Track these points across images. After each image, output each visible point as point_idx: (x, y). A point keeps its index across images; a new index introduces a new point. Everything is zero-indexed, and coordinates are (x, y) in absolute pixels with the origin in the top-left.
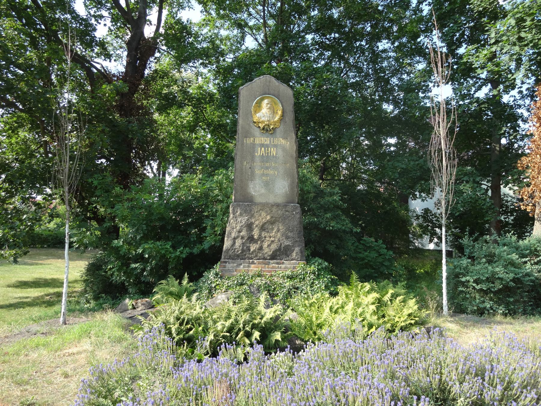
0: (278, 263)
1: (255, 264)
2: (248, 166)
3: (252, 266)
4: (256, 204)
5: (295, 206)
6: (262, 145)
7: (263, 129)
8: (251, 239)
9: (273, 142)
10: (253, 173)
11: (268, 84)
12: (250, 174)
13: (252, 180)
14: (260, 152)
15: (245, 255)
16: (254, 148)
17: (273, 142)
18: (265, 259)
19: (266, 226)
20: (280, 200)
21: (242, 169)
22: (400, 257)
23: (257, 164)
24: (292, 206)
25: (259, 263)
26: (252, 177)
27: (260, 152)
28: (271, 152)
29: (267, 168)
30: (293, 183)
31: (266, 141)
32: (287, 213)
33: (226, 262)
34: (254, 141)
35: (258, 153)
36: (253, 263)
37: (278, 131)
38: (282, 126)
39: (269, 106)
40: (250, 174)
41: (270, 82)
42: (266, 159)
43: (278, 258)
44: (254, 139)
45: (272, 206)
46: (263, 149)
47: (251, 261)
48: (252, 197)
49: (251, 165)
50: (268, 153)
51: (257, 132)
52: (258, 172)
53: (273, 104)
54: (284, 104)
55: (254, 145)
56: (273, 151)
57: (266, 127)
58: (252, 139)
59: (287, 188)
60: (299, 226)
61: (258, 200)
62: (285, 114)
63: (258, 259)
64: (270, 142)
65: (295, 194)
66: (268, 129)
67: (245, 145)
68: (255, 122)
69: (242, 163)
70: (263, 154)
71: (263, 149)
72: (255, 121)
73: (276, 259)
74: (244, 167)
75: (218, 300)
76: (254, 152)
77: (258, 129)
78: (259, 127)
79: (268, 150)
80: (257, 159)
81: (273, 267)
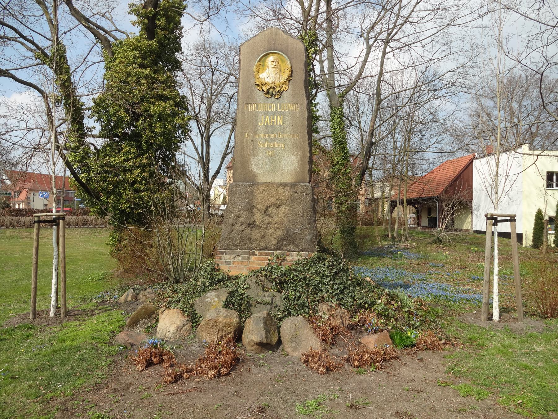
1: (256, 255)
2: (250, 139)
3: (252, 257)
4: (258, 184)
5: (305, 186)
6: (266, 113)
7: (268, 92)
8: (252, 225)
9: (280, 109)
10: (255, 146)
11: (273, 37)
12: (252, 148)
13: (254, 155)
14: (264, 121)
16: (256, 116)
17: (280, 109)
18: (266, 248)
19: (270, 210)
20: (288, 179)
21: (243, 143)
22: (288, 230)
25: (261, 255)
26: (255, 151)
27: (263, 121)
28: (277, 121)
29: (272, 141)
30: (304, 157)
31: (271, 107)
32: (296, 194)
33: (222, 253)
34: (257, 108)
35: (261, 122)
36: (254, 254)
39: (274, 64)
40: (252, 148)
41: (276, 35)
42: (271, 130)
43: (285, 248)
44: (257, 106)
45: (279, 185)
46: (268, 117)
47: (251, 252)
48: (254, 175)
49: (254, 137)
50: (273, 122)
51: (260, 96)
52: (261, 146)
53: (280, 61)
54: (293, 61)
55: (256, 112)
57: (271, 90)
58: (254, 106)
59: (296, 164)
60: (309, 210)
61: (262, 179)
64: (276, 108)
65: (307, 171)
66: (274, 93)
67: (246, 112)
68: (258, 85)
70: (267, 123)
71: (268, 117)
73: (282, 250)
74: (245, 140)
75: (208, 298)
76: (257, 121)
77: (259, 91)
78: (263, 90)
79: (273, 119)
80: (261, 131)
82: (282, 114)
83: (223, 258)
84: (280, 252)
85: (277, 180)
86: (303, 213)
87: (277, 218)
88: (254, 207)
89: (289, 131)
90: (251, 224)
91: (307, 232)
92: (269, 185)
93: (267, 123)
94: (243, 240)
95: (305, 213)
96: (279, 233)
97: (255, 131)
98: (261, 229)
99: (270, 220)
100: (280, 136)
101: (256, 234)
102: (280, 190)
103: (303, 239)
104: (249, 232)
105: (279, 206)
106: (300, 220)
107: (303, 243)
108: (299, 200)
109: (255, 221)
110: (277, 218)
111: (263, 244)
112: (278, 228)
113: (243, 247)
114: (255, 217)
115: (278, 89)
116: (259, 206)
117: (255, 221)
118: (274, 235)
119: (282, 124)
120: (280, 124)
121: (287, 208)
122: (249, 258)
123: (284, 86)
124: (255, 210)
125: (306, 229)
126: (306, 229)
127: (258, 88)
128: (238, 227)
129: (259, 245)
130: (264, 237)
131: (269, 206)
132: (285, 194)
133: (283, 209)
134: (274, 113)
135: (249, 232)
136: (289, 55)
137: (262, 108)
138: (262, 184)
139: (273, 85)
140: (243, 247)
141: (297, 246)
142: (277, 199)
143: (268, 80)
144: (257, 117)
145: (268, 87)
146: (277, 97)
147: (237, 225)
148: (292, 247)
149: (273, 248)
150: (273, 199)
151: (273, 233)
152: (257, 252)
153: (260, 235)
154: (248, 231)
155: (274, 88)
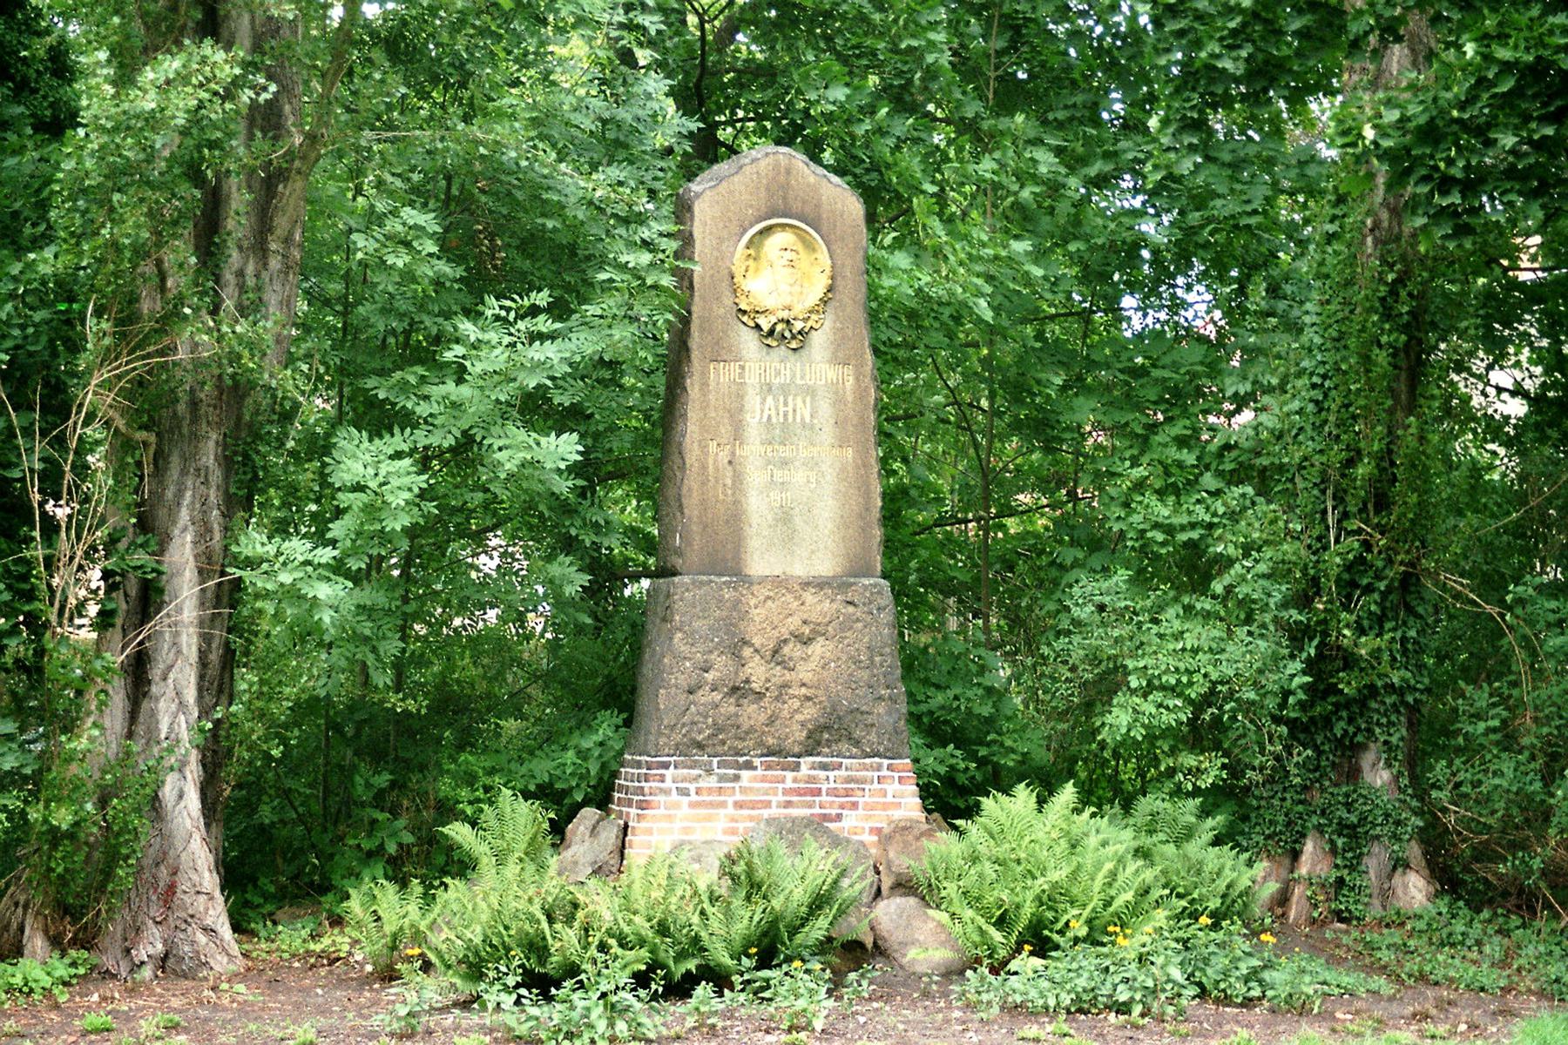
0: (824, 767)
1: (755, 768)
2: (724, 457)
3: (745, 774)
5: (875, 586)
7: (771, 332)
15: (723, 743)
16: (740, 397)
19: (786, 650)
20: (825, 565)
21: (704, 467)
23: (753, 450)
24: (865, 587)
25: (769, 767)
32: (851, 609)
33: (666, 766)
34: (741, 376)
36: (749, 766)
37: (818, 340)
38: (828, 324)
40: (729, 482)
41: (788, 172)
43: (826, 750)
44: (742, 367)
45: (806, 585)
46: (770, 399)
47: (741, 760)
49: (733, 454)
51: (748, 342)
54: (834, 247)
56: (802, 408)
57: (779, 327)
62: (839, 282)
63: (762, 755)
65: (875, 547)
66: (787, 334)
68: (744, 312)
69: (704, 448)
70: (769, 417)
72: (743, 307)
73: (818, 754)
74: (711, 461)
76: (741, 409)
78: (758, 327)
79: (786, 404)
81: (811, 780)
82: (810, 391)
83: (669, 779)
84: (818, 759)
85: (800, 570)
86: (871, 659)
87: (805, 672)
88: (746, 643)
89: (828, 435)
90: (738, 688)
91: (881, 709)
92: (780, 582)
93: (769, 417)
94: (718, 729)
95: (877, 659)
96: (810, 712)
97: (738, 434)
98: (766, 702)
99: (788, 677)
100: (804, 454)
101: (752, 714)
102: (809, 597)
103: (873, 725)
104: (732, 709)
105: (807, 642)
106: (865, 674)
107: (873, 737)
108: (860, 625)
109: (747, 681)
110: (805, 672)
111: (771, 741)
112: (808, 699)
113: (719, 749)
114: (748, 670)
115: (798, 325)
116: (757, 641)
117: (747, 681)
118: (799, 717)
119: (808, 420)
120: (802, 419)
121: (831, 645)
122: (737, 778)
123: (814, 317)
124: (747, 652)
125: (880, 698)
126: (880, 698)
127: (745, 319)
128: (705, 697)
129: (761, 744)
130: (771, 721)
131: (785, 641)
132: (819, 606)
133: (818, 648)
134: (785, 389)
135: (732, 709)
136: (824, 229)
137: (752, 379)
138: (763, 580)
139: (785, 315)
140: (719, 749)
141: (857, 743)
142: (805, 622)
143: (768, 303)
144: (742, 398)
145: (774, 320)
146: (794, 345)
147: (701, 692)
148: (844, 746)
149: (796, 749)
150: (794, 623)
151: (796, 711)
152: (757, 762)
153: (763, 718)
154: (729, 708)
155: (788, 322)
